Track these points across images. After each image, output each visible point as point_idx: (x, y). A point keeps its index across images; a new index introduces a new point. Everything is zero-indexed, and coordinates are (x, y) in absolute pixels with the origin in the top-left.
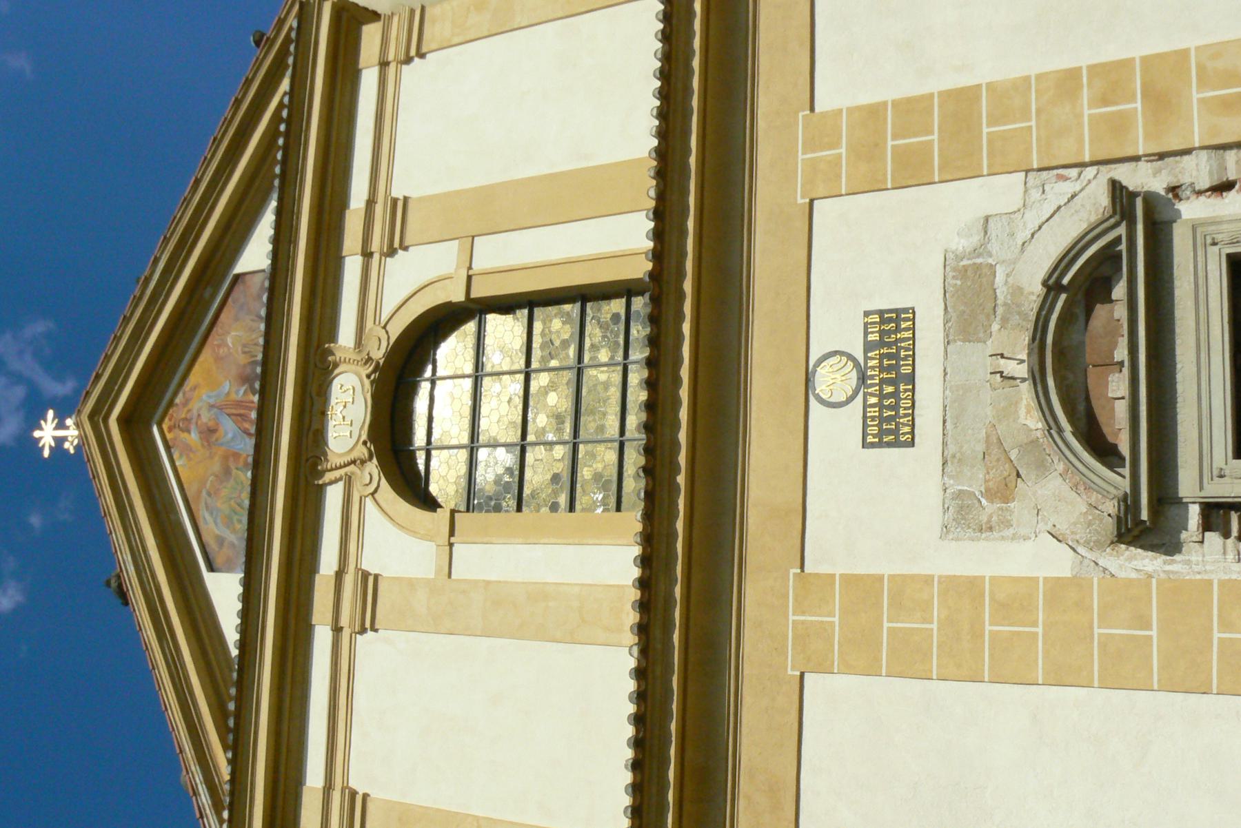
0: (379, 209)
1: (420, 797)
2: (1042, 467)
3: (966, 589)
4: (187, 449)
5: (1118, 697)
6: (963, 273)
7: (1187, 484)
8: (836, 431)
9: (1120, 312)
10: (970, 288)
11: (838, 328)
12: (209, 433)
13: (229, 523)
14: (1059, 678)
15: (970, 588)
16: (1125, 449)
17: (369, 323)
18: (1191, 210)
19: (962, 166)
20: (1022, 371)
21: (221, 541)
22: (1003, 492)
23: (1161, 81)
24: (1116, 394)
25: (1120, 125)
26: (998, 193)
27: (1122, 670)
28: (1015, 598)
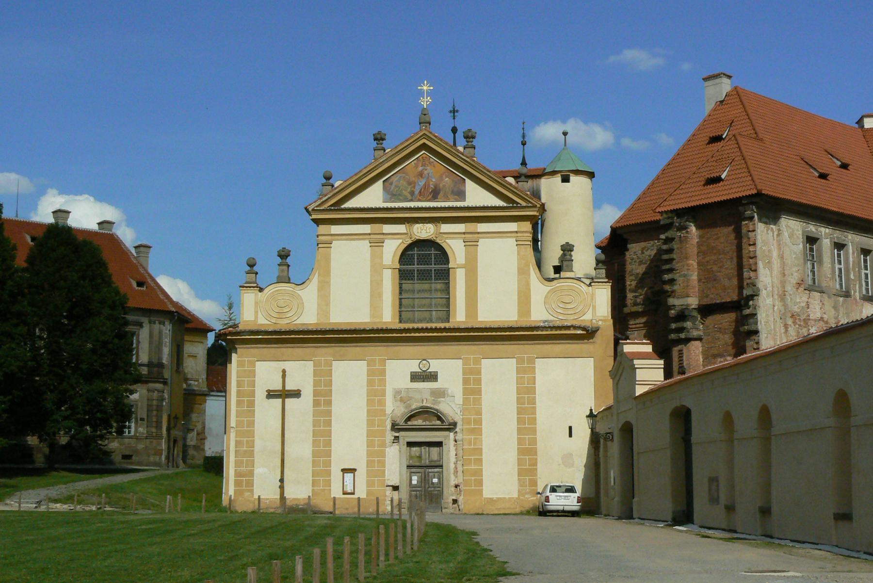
0: (476, 235)
1: (334, 265)
2: (406, 407)
3: (383, 394)
4: (417, 166)
5: (366, 422)
6: (444, 391)
7: (402, 434)
8: (414, 366)
9: (434, 423)
10: (440, 394)
11: (435, 365)
12: (421, 174)
13: (396, 186)
14: (368, 411)
15: (384, 394)
16: (409, 423)
17: (445, 236)
18: (452, 434)
19: (466, 392)
20: (424, 404)
21: (391, 184)
22: (401, 400)
23: (477, 431)
24: (418, 422)
25: (469, 423)
26: (459, 399)
27: (370, 423)
28: (382, 403)
